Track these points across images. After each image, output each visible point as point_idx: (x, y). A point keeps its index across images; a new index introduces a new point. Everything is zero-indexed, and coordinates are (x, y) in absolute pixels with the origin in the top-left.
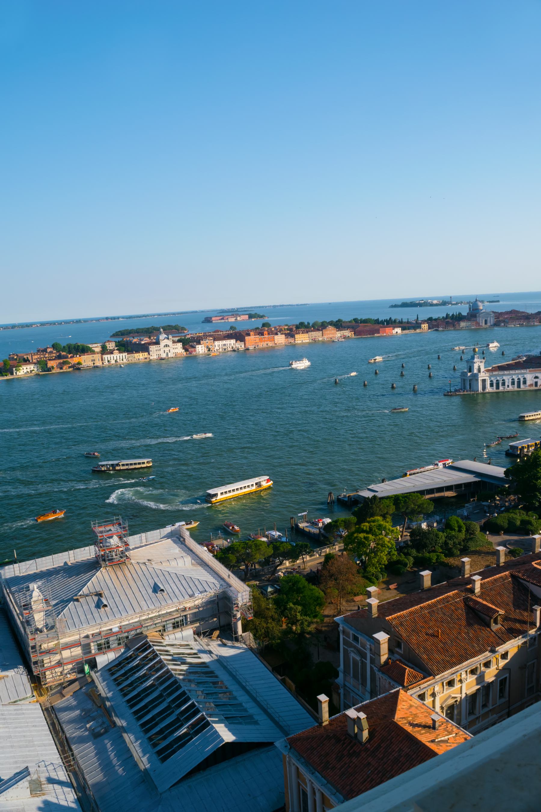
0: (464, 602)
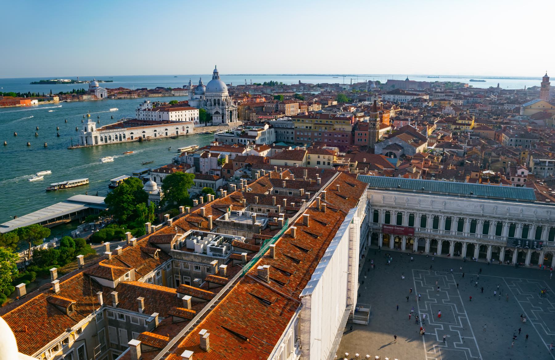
0: (47, 301)
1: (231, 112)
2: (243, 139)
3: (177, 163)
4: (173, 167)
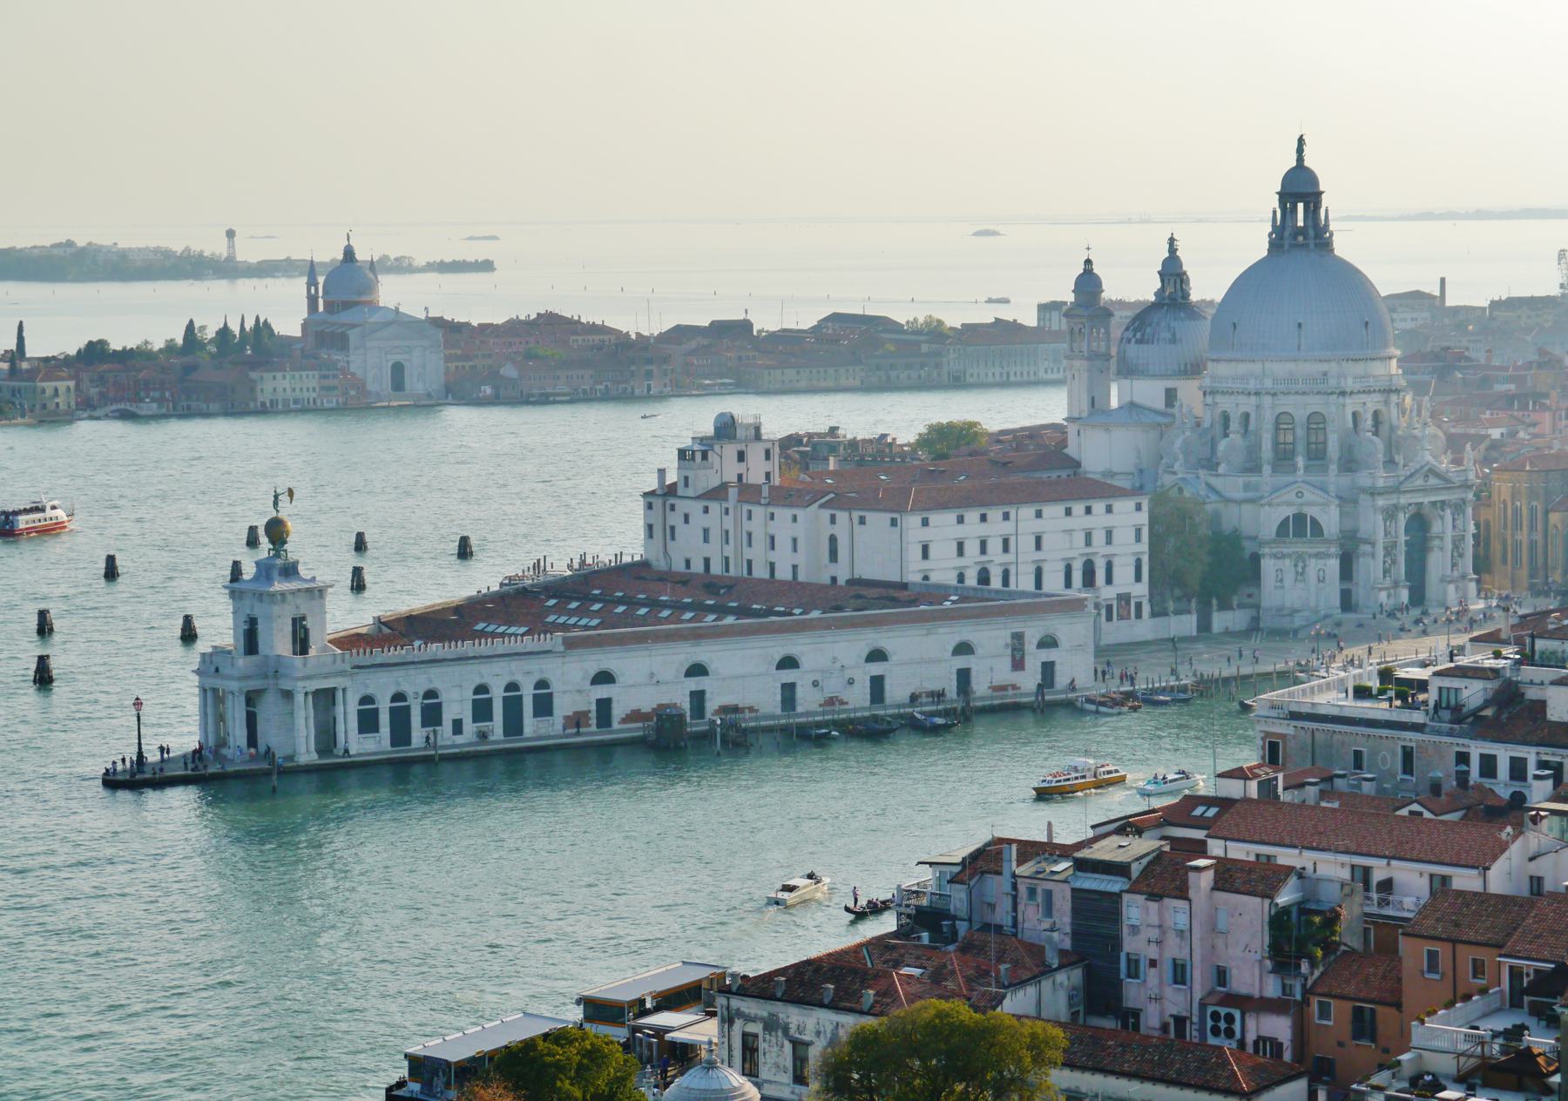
1: (1419, 524)
2: (1504, 754)
3: (935, 930)
4: (897, 964)
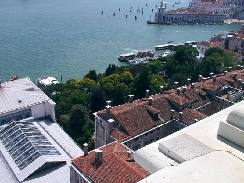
4: (211, 43)
